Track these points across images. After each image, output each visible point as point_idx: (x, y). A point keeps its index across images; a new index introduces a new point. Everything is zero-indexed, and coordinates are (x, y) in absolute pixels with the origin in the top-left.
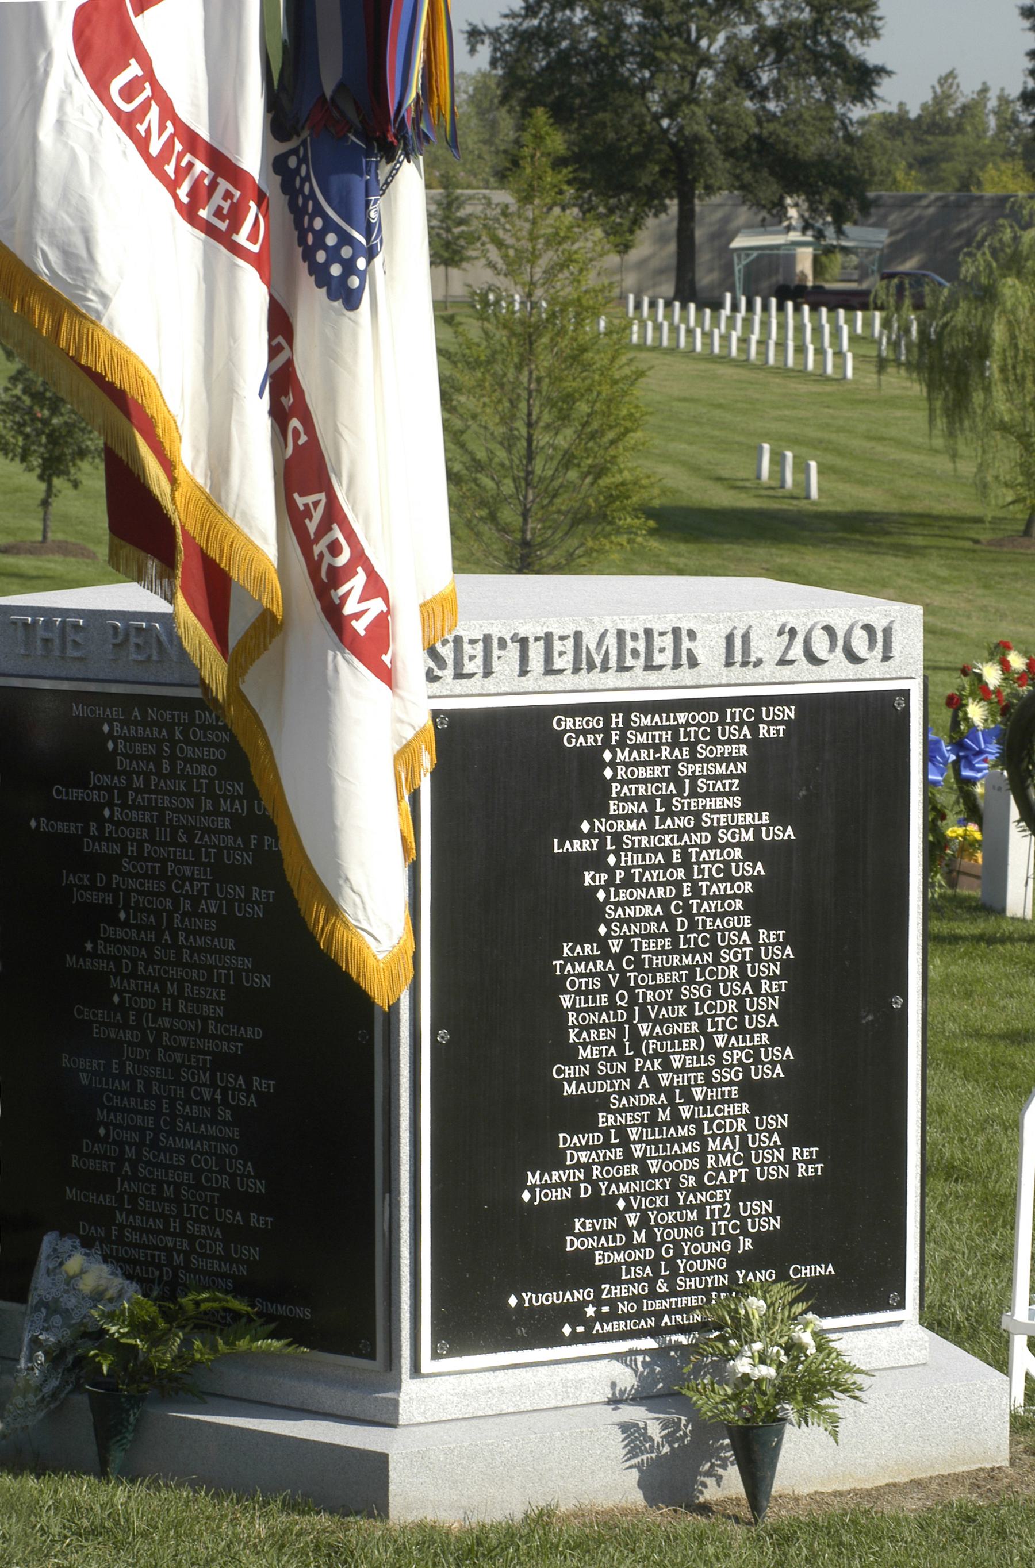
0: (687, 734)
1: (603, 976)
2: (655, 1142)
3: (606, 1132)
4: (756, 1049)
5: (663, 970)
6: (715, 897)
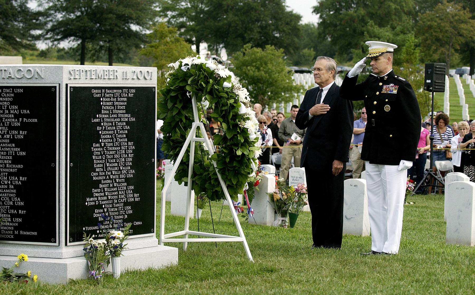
2: (110, 192)
3: (101, 189)
5: (111, 151)
6: (121, 134)
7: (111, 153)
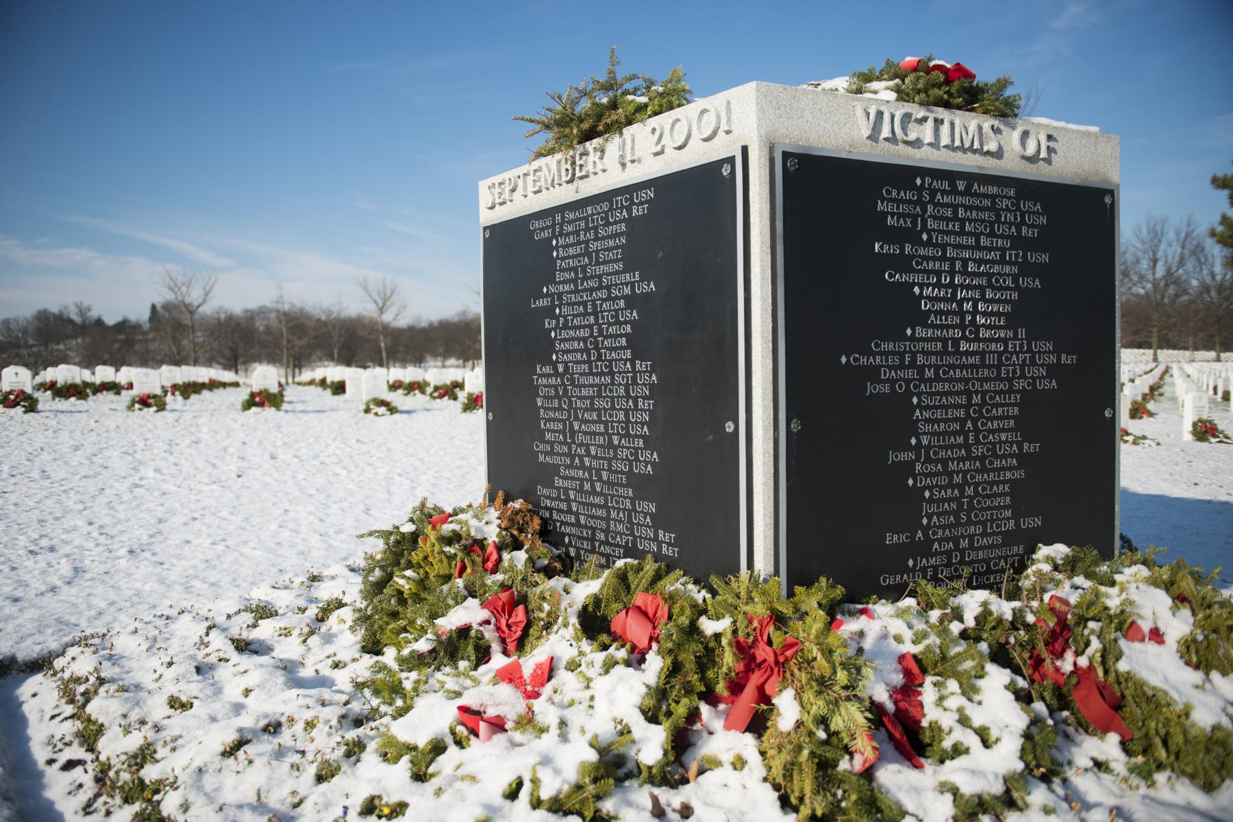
0: (593, 221)
1: (555, 387)
3: (558, 489)
4: (636, 449)
5: (585, 386)
6: (611, 336)
7: (584, 392)
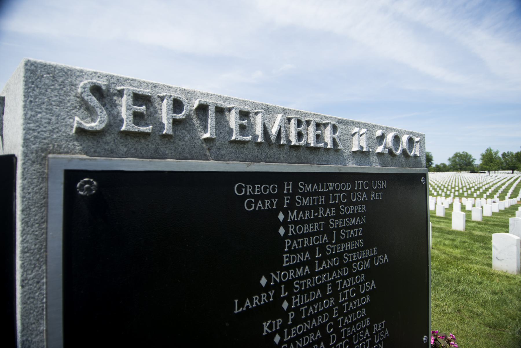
0: (334, 198)
